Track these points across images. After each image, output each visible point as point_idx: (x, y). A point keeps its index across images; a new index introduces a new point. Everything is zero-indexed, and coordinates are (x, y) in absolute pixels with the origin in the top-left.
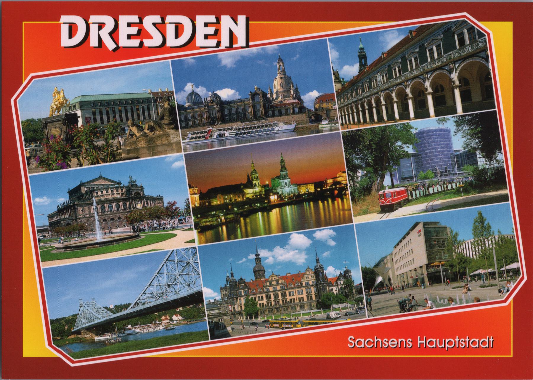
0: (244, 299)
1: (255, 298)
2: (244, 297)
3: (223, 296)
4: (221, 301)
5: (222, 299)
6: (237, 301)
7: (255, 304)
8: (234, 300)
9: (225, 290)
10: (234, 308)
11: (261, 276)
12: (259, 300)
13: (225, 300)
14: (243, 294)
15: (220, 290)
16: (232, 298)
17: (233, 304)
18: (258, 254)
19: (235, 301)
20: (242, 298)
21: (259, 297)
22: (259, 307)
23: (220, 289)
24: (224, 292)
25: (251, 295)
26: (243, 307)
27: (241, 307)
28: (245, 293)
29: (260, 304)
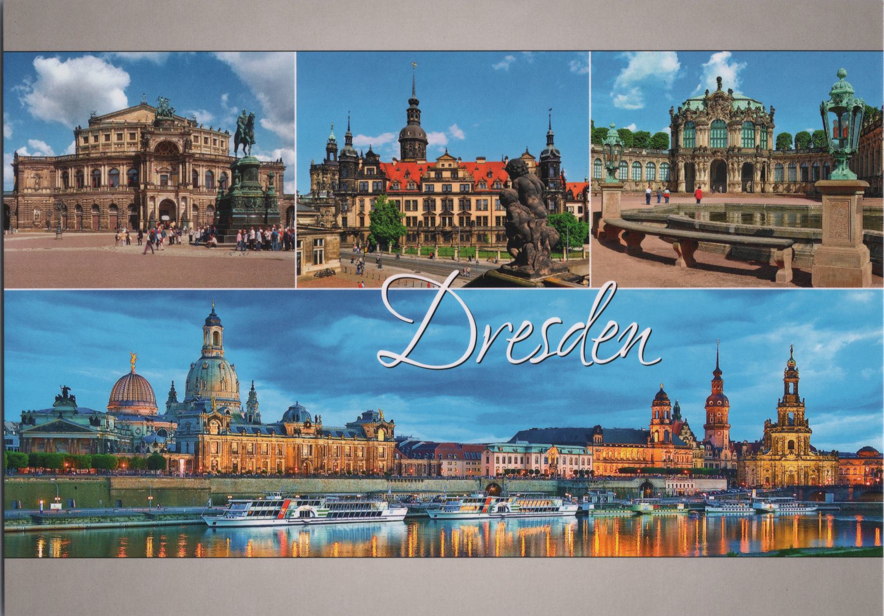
0: (371, 200)
1: (398, 201)
2: (372, 197)
3: (315, 187)
4: (311, 197)
5: (313, 192)
6: (354, 204)
7: (398, 218)
8: (346, 200)
9: (323, 174)
10: (343, 218)
11: (417, 155)
12: (408, 208)
13: (321, 197)
14: (370, 190)
15: (311, 170)
16: (344, 195)
17: (342, 210)
18: (416, 100)
19: (349, 202)
20: (367, 201)
21: (408, 202)
22: (404, 224)
23: (310, 168)
24: (320, 177)
25: (390, 195)
26: (368, 222)
27: (362, 219)
28: (375, 188)
29: (408, 218)
